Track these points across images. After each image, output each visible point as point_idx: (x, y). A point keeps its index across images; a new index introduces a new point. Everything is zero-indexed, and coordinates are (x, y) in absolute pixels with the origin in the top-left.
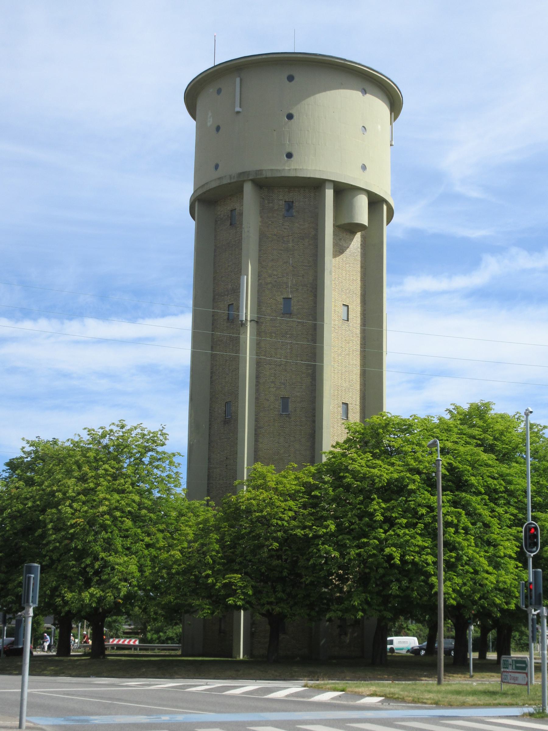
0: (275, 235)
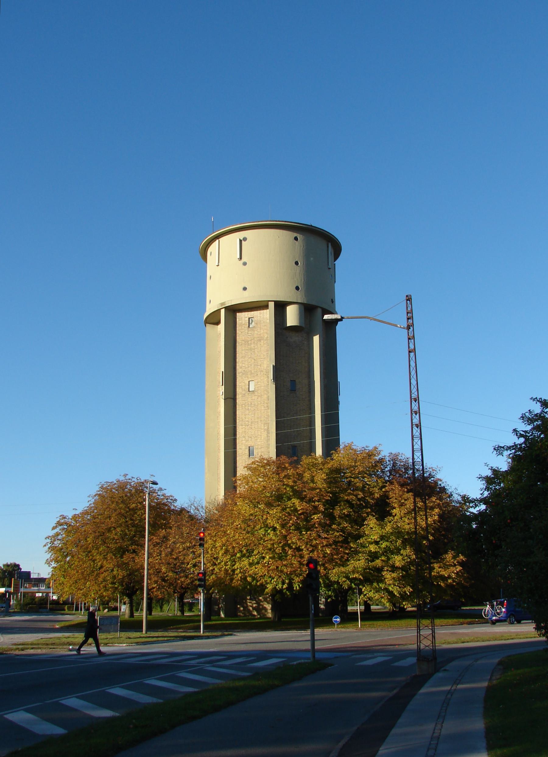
0: (243, 341)
